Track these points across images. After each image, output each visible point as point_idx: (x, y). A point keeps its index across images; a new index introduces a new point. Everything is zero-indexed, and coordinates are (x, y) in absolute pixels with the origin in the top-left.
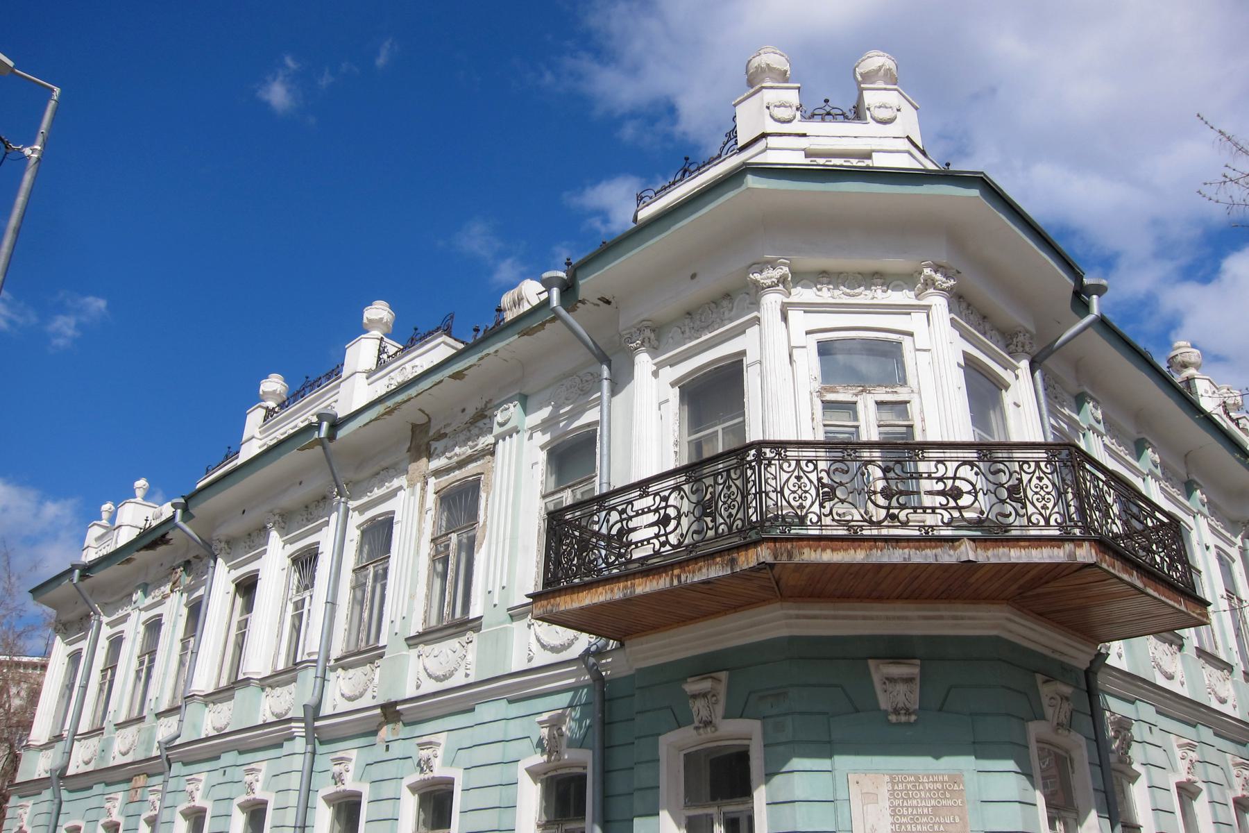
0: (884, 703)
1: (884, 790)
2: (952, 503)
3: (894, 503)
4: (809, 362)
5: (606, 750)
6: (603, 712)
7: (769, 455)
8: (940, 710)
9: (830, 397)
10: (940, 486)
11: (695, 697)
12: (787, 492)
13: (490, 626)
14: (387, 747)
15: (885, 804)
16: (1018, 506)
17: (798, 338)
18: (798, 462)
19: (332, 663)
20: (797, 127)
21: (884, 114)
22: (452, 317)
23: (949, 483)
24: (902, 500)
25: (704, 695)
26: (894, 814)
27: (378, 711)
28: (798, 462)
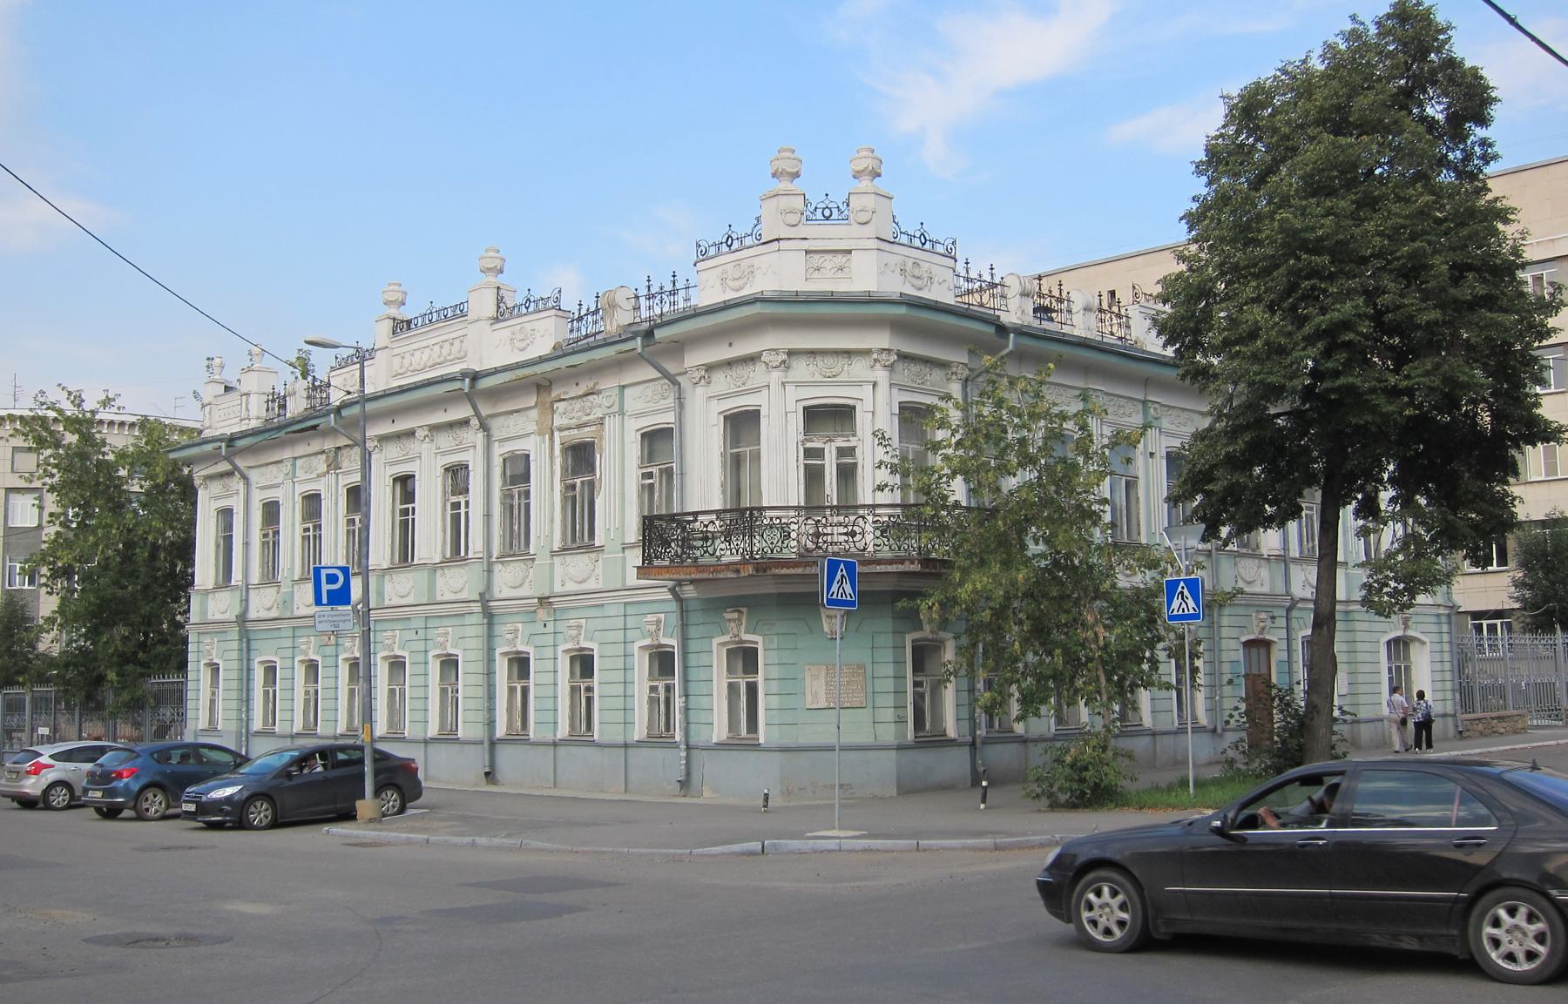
0: (826, 629)
1: (824, 672)
2: (851, 539)
3: (820, 540)
4: (797, 421)
5: (684, 640)
6: (682, 619)
7: (756, 515)
8: (857, 631)
9: (809, 445)
10: (845, 530)
11: (729, 620)
12: (765, 536)
13: (610, 553)
14: (545, 625)
15: (823, 680)
16: (885, 540)
17: (791, 406)
18: (771, 519)
19: (494, 559)
20: (802, 231)
21: (863, 217)
22: (560, 291)
23: (850, 528)
24: (825, 538)
25: (734, 620)
26: (827, 685)
27: (536, 601)
28: (771, 519)
